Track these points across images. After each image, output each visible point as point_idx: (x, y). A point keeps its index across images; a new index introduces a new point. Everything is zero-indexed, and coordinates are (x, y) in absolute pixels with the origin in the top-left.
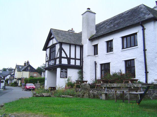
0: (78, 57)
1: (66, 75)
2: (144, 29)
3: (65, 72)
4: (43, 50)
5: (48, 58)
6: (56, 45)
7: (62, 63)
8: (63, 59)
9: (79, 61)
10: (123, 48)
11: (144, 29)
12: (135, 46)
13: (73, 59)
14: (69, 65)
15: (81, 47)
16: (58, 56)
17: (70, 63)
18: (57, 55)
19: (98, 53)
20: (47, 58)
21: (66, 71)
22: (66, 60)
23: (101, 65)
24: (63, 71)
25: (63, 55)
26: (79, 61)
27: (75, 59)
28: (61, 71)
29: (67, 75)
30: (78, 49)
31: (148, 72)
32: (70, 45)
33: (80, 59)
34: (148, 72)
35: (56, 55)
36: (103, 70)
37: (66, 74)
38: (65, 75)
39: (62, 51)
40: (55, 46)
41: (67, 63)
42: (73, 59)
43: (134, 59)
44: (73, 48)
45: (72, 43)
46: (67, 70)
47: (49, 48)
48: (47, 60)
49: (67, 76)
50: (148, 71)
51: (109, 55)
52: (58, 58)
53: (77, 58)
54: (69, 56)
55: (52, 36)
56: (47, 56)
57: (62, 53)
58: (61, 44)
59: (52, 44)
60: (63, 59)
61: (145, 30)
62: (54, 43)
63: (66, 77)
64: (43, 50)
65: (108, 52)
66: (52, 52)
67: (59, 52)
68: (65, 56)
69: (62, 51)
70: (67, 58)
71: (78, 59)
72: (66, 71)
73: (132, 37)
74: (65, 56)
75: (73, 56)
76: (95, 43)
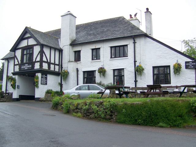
0: (57, 62)
2: (134, 43)
3: (45, 77)
6: (35, 47)
8: (44, 64)
10: (111, 57)
11: (134, 43)
12: (124, 56)
13: (52, 64)
14: (49, 70)
15: (61, 51)
16: (38, 59)
18: (36, 58)
22: (47, 64)
23: (84, 72)
24: (43, 77)
25: (44, 59)
26: (58, 66)
27: (55, 64)
28: (42, 77)
29: (47, 81)
30: (57, 54)
31: (137, 81)
32: (51, 48)
33: (59, 65)
34: (137, 81)
36: (85, 78)
38: (45, 81)
39: (44, 54)
42: (52, 64)
43: (123, 69)
44: (53, 52)
45: (52, 46)
47: (21, 50)
50: (137, 80)
52: (38, 62)
53: (56, 63)
54: (49, 61)
58: (42, 46)
59: (27, 45)
60: (44, 64)
61: (136, 44)
62: (29, 44)
65: (92, 59)
67: (39, 55)
68: (46, 61)
69: (44, 54)
70: (47, 62)
71: (57, 65)
73: (122, 48)
74: (46, 61)
75: (52, 61)
76: (77, 49)
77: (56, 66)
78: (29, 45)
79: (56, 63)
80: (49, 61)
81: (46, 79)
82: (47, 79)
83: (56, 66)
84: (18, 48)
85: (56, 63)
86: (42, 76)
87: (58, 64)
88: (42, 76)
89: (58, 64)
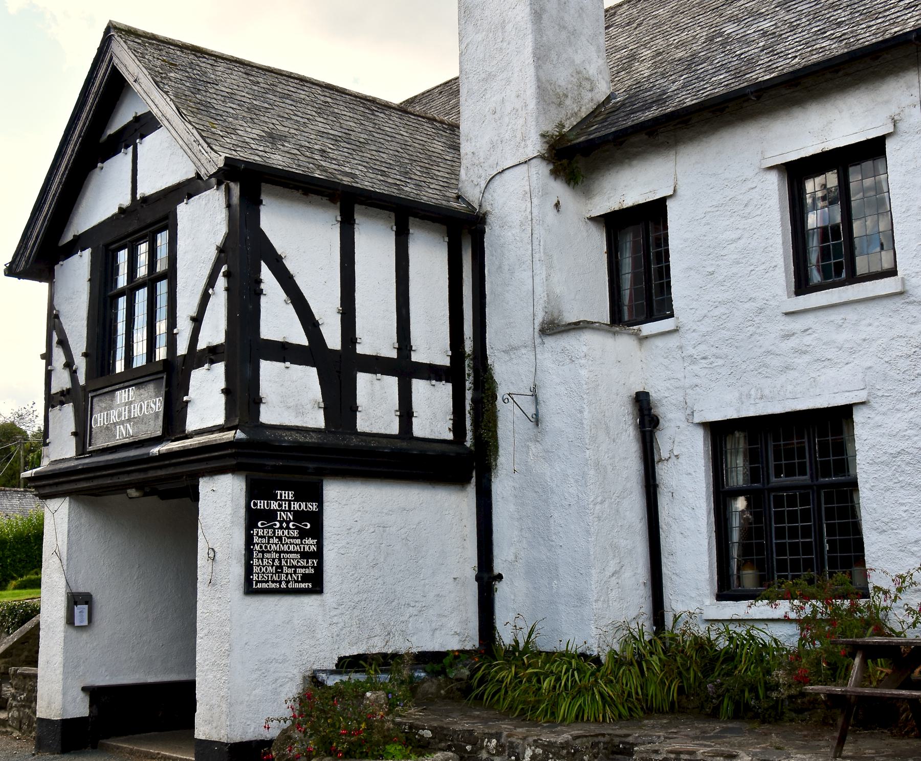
1: (305, 555)
3: (299, 516)
4: (12, 271)
5: (81, 363)
6: (184, 211)
7: (268, 415)
8: (268, 369)
9: (445, 389)
13: (376, 365)
14: (340, 441)
17: (354, 409)
18: (197, 321)
19: (676, 304)
20: (59, 357)
21: (313, 507)
24: (270, 516)
26: (445, 389)
28: (253, 518)
29: (318, 554)
35: (184, 328)
37: (310, 544)
38: (294, 559)
39: (266, 273)
40: (169, 223)
41: (317, 420)
42: (376, 365)
45: (368, 182)
46: (319, 499)
47: (87, 253)
48: (62, 381)
49: (319, 569)
51: (835, 316)
52: (212, 354)
53: (419, 356)
54: (333, 339)
55: (123, 117)
56: (63, 343)
57: (263, 300)
59: (126, 201)
60: (268, 369)
62: (146, 188)
63: (305, 578)
64: (12, 271)
65: (802, 286)
66: (130, 292)
67: (221, 283)
68: (299, 337)
69: (266, 273)
71: (432, 372)
72: (313, 507)
74: (299, 337)
77: (419, 387)
78: (145, 199)
79: (415, 358)
80: (333, 339)
81: (303, 534)
82: (317, 532)
83: (419, 387)
84: (68, 237)
85: (415, 358)
86: (261, 504)
87: (444, 360)
88: (261, 504)
89: (444, 360)
